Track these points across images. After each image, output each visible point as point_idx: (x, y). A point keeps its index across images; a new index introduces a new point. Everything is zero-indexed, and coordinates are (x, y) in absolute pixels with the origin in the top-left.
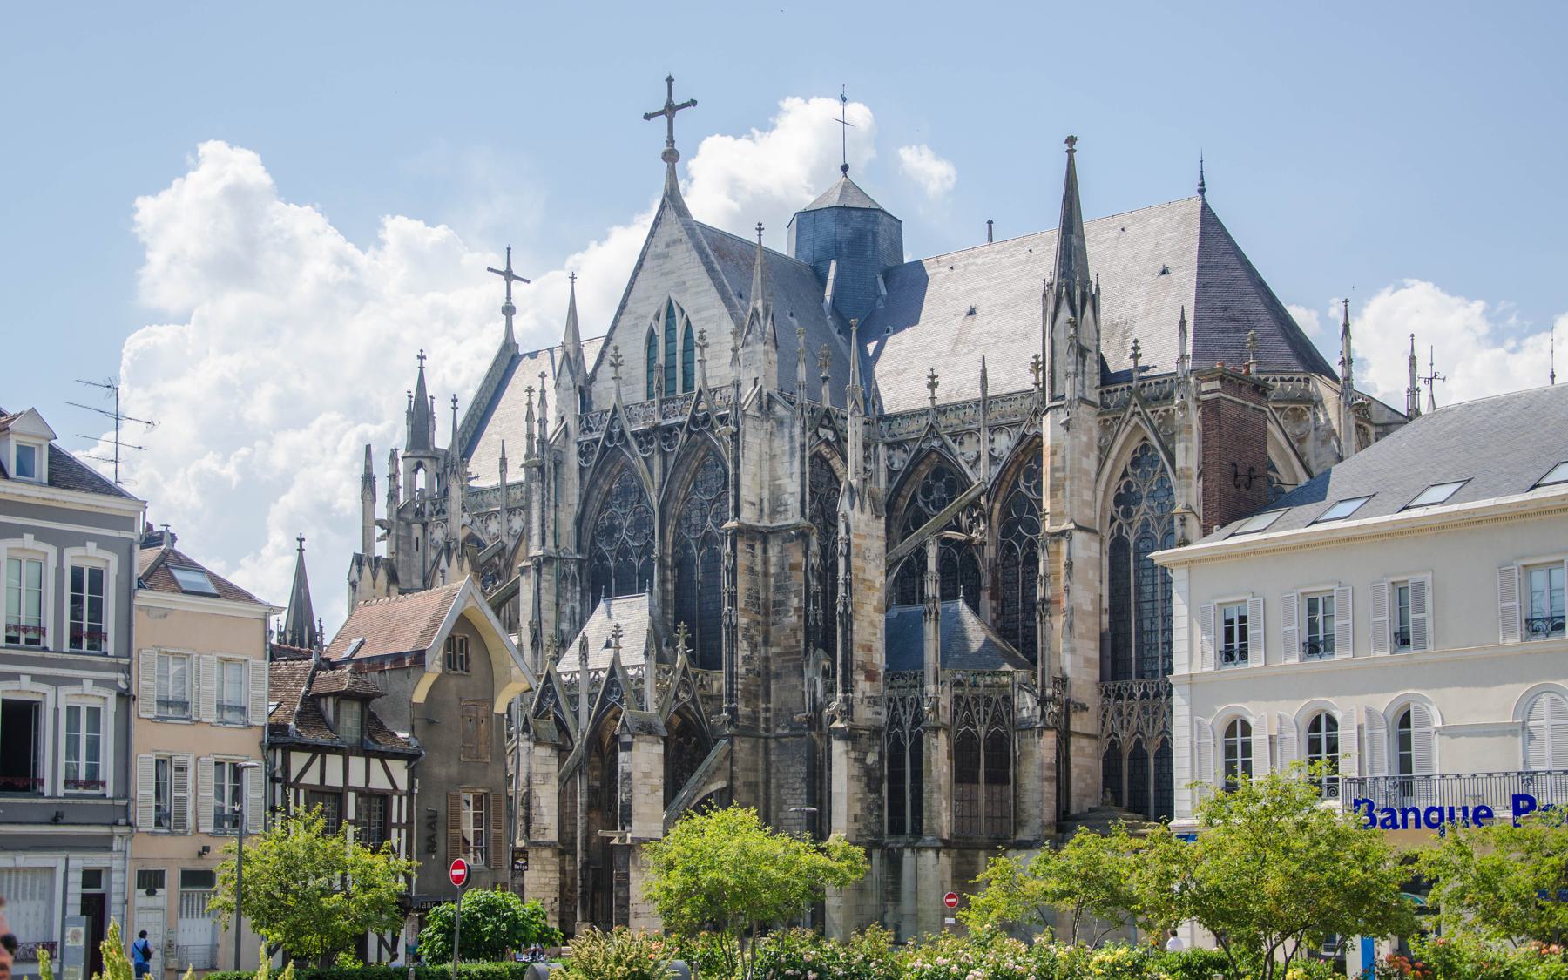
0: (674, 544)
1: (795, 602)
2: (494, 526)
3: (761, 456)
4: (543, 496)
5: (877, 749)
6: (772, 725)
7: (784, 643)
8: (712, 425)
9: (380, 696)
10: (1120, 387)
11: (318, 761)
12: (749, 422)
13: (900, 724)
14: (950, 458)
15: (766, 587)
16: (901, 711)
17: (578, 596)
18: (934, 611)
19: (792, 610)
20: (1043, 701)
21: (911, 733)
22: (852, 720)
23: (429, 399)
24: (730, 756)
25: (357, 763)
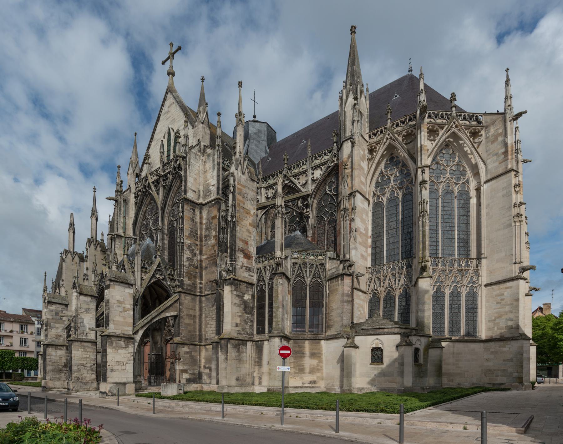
1: (214, 233)
5: (251, 293)
7: (209, 253)
13: (263, 280)
16: (264, 273)
19: (212, 237)
22: (235, 275)
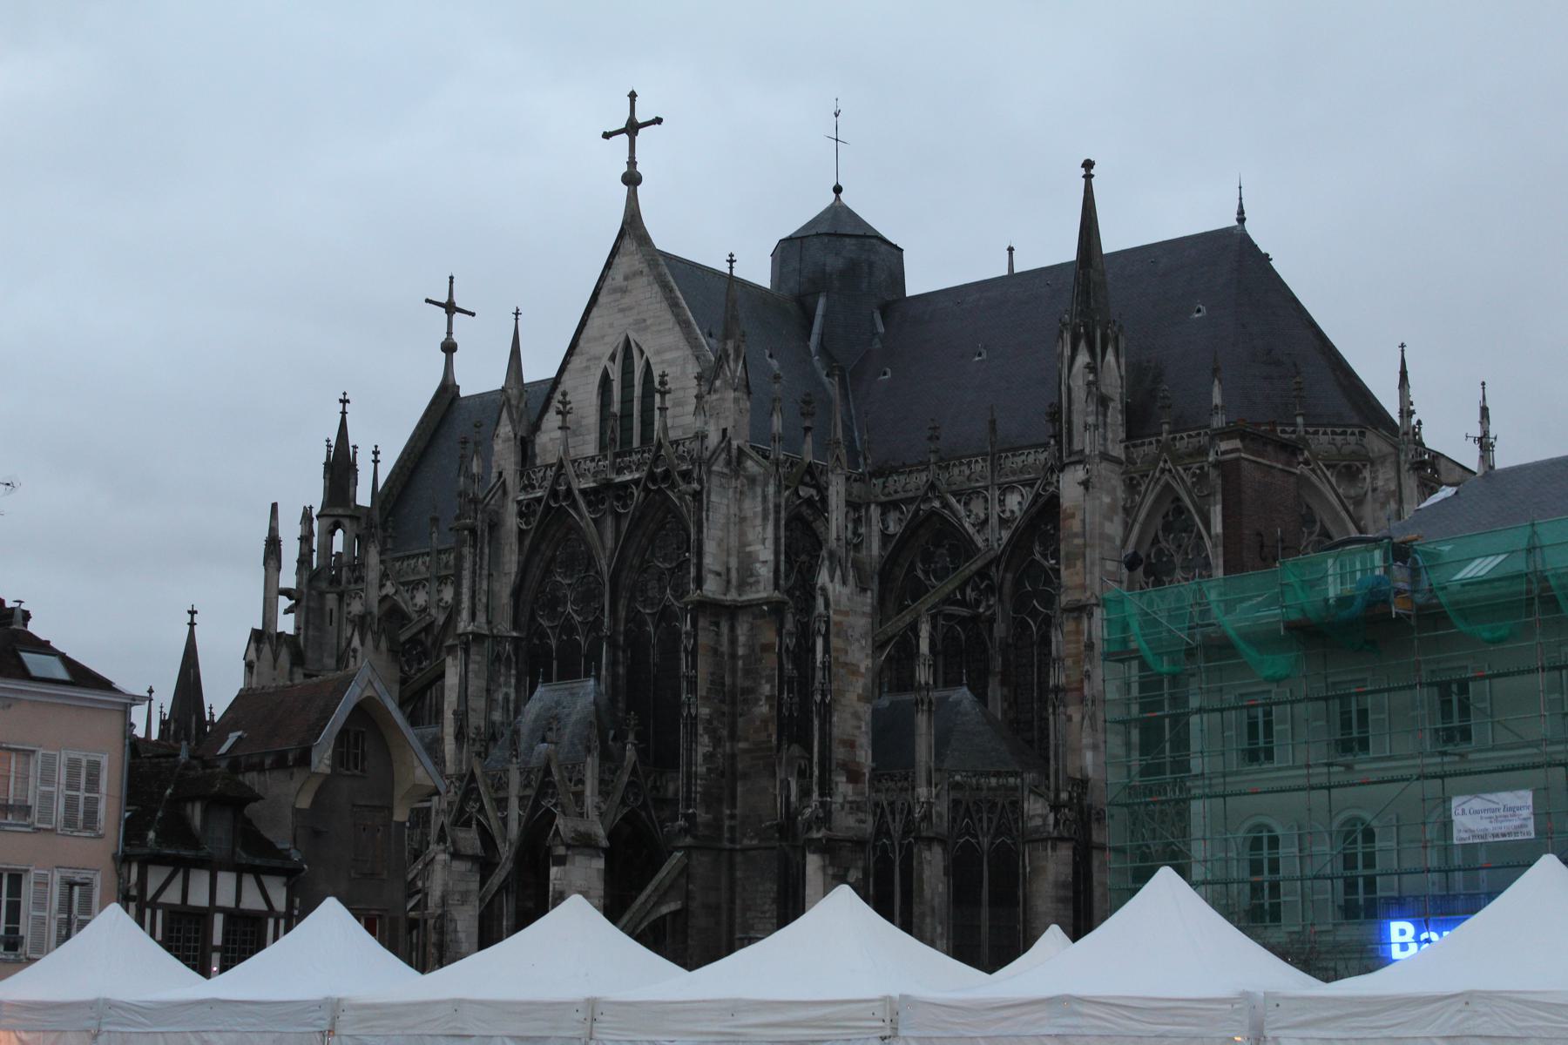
0: (627, 621)
2: (421, 598)
3: (729, 519)
4: (475, 564)
5: (860, 864)
6: (738, 835)
8: (673, 483)
9: (257, 798)
10: (1147, 440)
11: (179, 879)
12: (715, 481)
13: (888, 834)
14: (953, 520)
15: (734, 671)
16: (889, 818)
17: (513, 681)
18: (926, 700)
19: (763, 698)
20: (1056, 807)
21: (901, 845)
23: (351, 449)
24: (685, 872)
25: (226, 881)
